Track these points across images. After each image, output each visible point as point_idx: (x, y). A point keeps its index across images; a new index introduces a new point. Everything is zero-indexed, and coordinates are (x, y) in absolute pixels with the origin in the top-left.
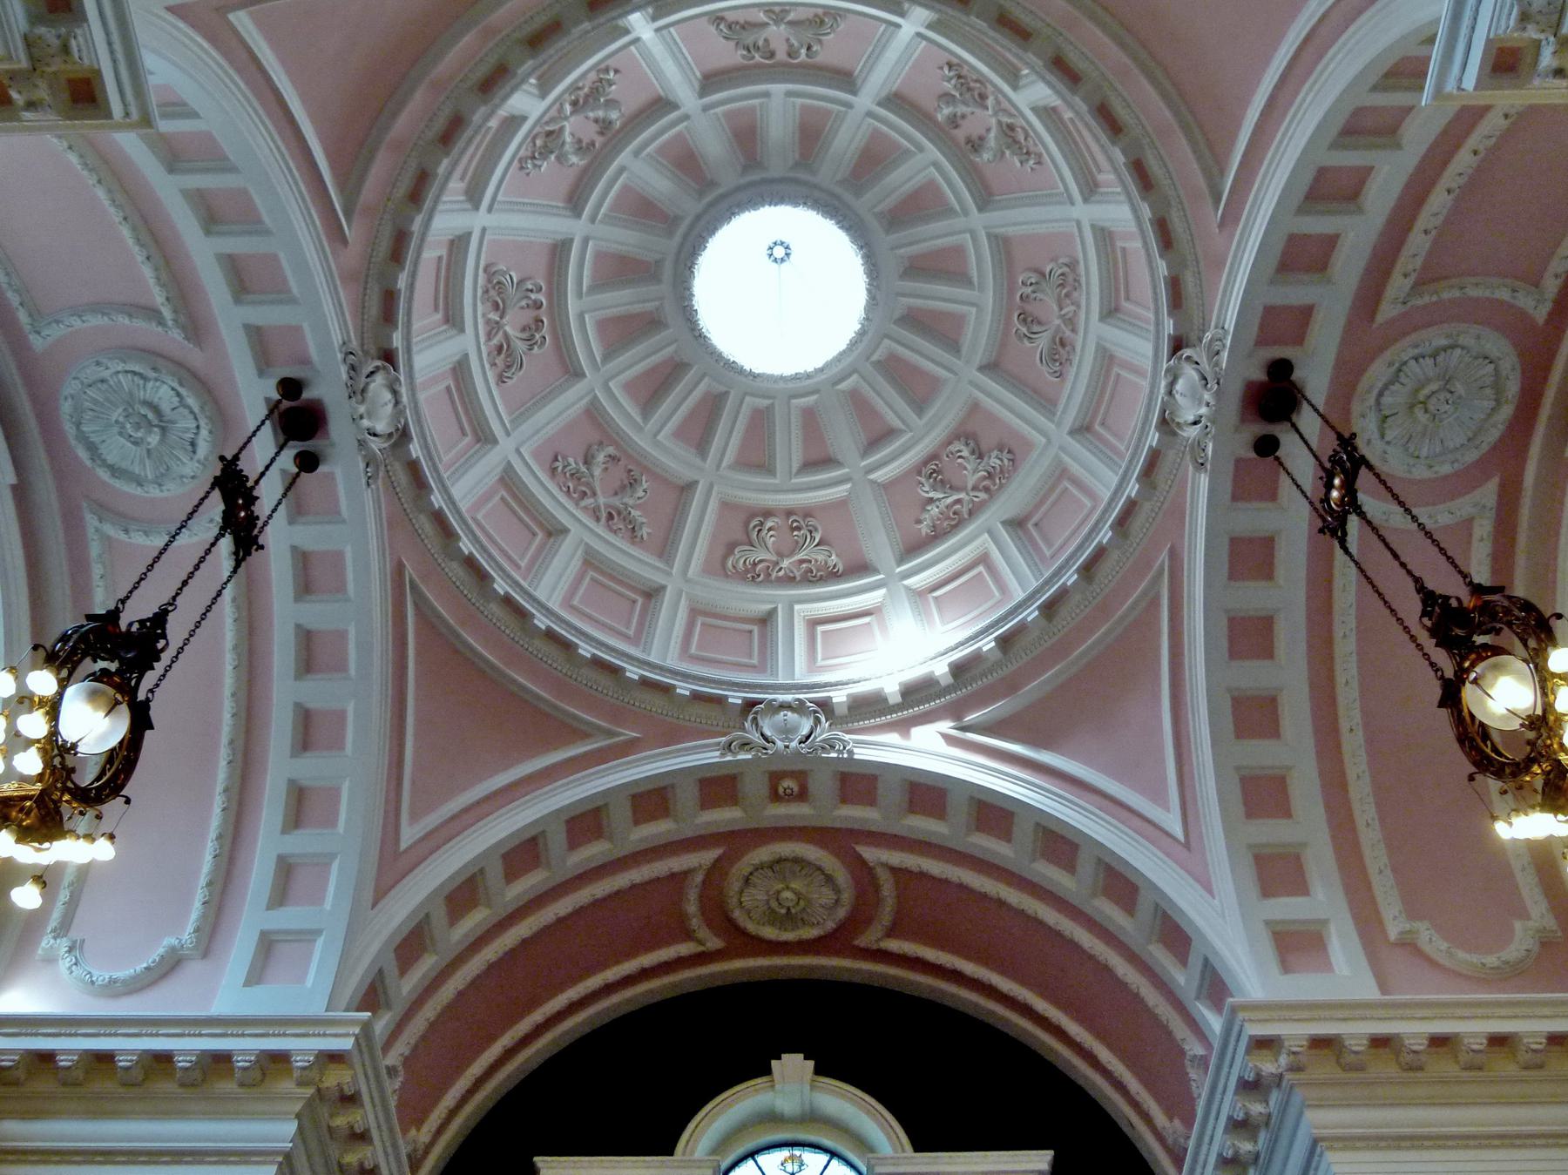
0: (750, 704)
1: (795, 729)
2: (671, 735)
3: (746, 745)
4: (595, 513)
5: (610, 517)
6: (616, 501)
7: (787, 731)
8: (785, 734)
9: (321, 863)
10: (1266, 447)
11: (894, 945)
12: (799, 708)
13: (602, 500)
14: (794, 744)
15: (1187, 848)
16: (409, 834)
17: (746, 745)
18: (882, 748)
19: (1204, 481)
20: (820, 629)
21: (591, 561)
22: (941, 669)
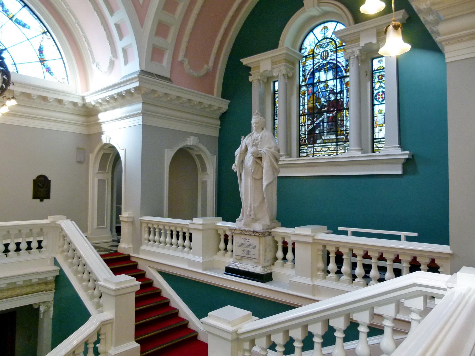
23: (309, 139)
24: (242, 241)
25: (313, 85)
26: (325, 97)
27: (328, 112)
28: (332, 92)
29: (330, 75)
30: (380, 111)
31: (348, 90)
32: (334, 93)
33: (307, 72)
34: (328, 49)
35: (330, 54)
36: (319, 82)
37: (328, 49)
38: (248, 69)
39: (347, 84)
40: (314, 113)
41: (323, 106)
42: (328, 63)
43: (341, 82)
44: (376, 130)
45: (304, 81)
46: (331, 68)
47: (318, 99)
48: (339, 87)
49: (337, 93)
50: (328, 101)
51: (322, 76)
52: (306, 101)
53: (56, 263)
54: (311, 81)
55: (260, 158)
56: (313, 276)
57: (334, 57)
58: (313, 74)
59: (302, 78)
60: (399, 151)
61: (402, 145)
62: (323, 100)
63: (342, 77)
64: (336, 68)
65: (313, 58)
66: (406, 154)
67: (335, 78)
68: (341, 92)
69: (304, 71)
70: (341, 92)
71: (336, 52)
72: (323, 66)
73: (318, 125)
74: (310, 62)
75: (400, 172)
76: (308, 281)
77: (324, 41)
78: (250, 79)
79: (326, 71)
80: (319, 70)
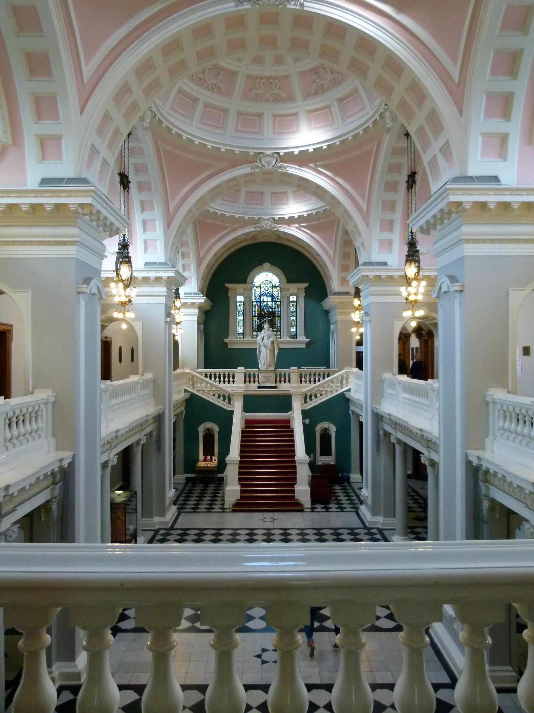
0: (259, 218)
1: (268, 224)
7: (267, 225)
8: (266, 225)
9: (189, 265)
12: (269, 219)
18: (285, 229)
22: (296, 216)
23: (258, 329)
24: (265, 375)
25: (260, 302)
26: (267, 309)
27: (268, 317)
28: (270, 307)
29: (269, 299)
30: (293, 320)
31: (278, 308)
32: (271, 308)
33: (257, 295)
34: (268, 286)
35: (270, 289)
36: (264, 301)
37: (268, 286)
38: (227, 289)
39: (278, 305)
41: (265, 314)
42: (268, 293)
43: (275, 304)
44: (291, 328)
45: (256, 299)
46: (270, 296)
47: (263, 310)
49: (273, 309)
50: (268, 311)
51: (265, 298)
53: (186, 391)
54: (259, 300)
55: (273, 343)
56: (298, 383)
58: (260, 296)
59: (253, 298)
61: (306, 336)
64: (272, 296)
65: (260, 288)
66: (308, 340)
67: (272, 301)
68: (275, 308)
69: (255, 294)
70: (275, 308)
71: (272, 288)
74: (258, 290)
76: (296, 385)
78: (229, 295)
79: (268, 296)
80: (264, 295)
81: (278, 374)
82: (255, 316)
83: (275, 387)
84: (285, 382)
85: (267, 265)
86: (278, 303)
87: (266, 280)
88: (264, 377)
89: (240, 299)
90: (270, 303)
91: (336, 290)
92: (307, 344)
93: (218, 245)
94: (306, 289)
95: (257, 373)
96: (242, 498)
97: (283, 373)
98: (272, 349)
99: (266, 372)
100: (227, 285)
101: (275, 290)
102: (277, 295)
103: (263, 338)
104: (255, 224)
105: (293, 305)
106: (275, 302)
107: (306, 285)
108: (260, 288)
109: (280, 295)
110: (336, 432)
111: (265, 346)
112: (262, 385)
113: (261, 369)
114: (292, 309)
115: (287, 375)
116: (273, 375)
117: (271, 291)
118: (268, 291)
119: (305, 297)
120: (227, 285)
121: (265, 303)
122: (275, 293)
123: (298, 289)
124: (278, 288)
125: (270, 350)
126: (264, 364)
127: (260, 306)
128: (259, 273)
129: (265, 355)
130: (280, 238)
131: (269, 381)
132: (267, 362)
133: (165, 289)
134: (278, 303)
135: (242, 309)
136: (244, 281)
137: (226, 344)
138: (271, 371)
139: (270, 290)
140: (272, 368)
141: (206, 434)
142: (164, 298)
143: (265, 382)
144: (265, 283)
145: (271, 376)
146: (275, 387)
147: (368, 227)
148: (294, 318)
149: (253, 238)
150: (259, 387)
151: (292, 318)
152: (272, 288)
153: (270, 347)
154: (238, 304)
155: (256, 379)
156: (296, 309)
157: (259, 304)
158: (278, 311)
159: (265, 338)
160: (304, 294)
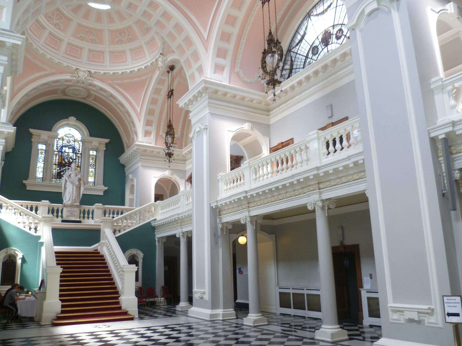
2: (61, 73)
3: (75, 77)
4: (53, 24)
5: (56, 25)
6: (57, 22)
10: (168, 72)
11: (92, 101)
13: (54, 21)
14: (83, 78)
15: (139, 115)
16: (16, 88)
17: (75, 77)
19: (158, 72)
20: (92, 53)
21: (50, 34)
23: (57, 176)
25: (62, 152)
28: (71, 158)
29: (71, 150)
30: (92, 171)
31: (78, 160)
32: (72, 159)
33: (59, 146)
34: (71, 139)
35: (72, 142)
36: (65, 152)
37: (71, 139)
38: (31, 135)
39: (78, 157)
40: (61, 165)
42: (70, 145)
43: (76, 156)
47: (64, 160)
48: (75, 157)
49: (73, 159)
51: (67, 150)
52: (57, 158)
54: (60, 150)
55: (80, 180)
57: (73, 143)
58: (62, 147)
59: (55, 148)
60: (104, 186)
61: (105, 184)
62: (66, 160)
63: (76, 153)
64: (74, 149)
65: (63, 140)
66: (106, 188)
67: (73, 152)
68: (75, 159)
69: (57, 144)
70: (75, 159)
71: (74, 142)
72: (68, 146)
73: (63, 171)
75: (103, 194)
77: (69, 135)
78: (33, 140)
79: (69, 148)
80: (65, 146)
81: (82, 210)
82: (55, 164)
83: (80, 222)
84: (88, 218)
85: (72, 119)
86: (79, 155)
87: (69, 133)
88: (68, 211)
89: (42, 147)
90: (71, 154)
91: (140, 141)
92: (105, 192)
93: (34, 85)
94: (106, 144)
95: (60, 209)
96: (63, 312)
97: (87, 210)
98: (79, 186)
99: (71, 206)
100: (32, 130)
101: (76, 143)
102: (78, 148)
103: (70, 176)
104: (72, 73)
105: (93, 158)
106: (76, 153)
107: (107, 141)
108: (63, 140)
109: (81, 148)
110: (143, 258)
111: (72, 183)
112: (65, 218)
113: (66, 204)
114: (91, 161)
115: (91, 212)
116: (77, 210)
117: (73, 143)
118: (71, 144)
119: (105, 151)
120: (32, 130)
121: (66, 154)
122: (77, 146)
123: (99, 144)
124: (80, 142)
125: (77, 187)
126: (69, 200)
127: (61, 156)
128: (62, 126)
129: (71, 191)
130: (89, 95)
131: (74, 216)
132: (73, 197)
133: (6, 58)
134: (79, 155)
135: (43, 156)
136: (50, 129)
137: (24, 186)
138: (77, 206)
139: (72, 143)
140: (78, 204)
141: (7, 260)
142: (3, 68)
143: (69, 216)
144: (67, 137)
145: (76, 211)
146: (80, 222)
147: (207, 52)
148: (93, 170)
149: (63, 92)
150: (63, 221)
151: (90, 170)
152: (74, 142)
153: (77, 183)
154: (40, 151)
155: (60, 214)
156: (95, 162)
157: (60, 153)
158: (78, 162)
159: (72, 175)
160: (105, 149)
